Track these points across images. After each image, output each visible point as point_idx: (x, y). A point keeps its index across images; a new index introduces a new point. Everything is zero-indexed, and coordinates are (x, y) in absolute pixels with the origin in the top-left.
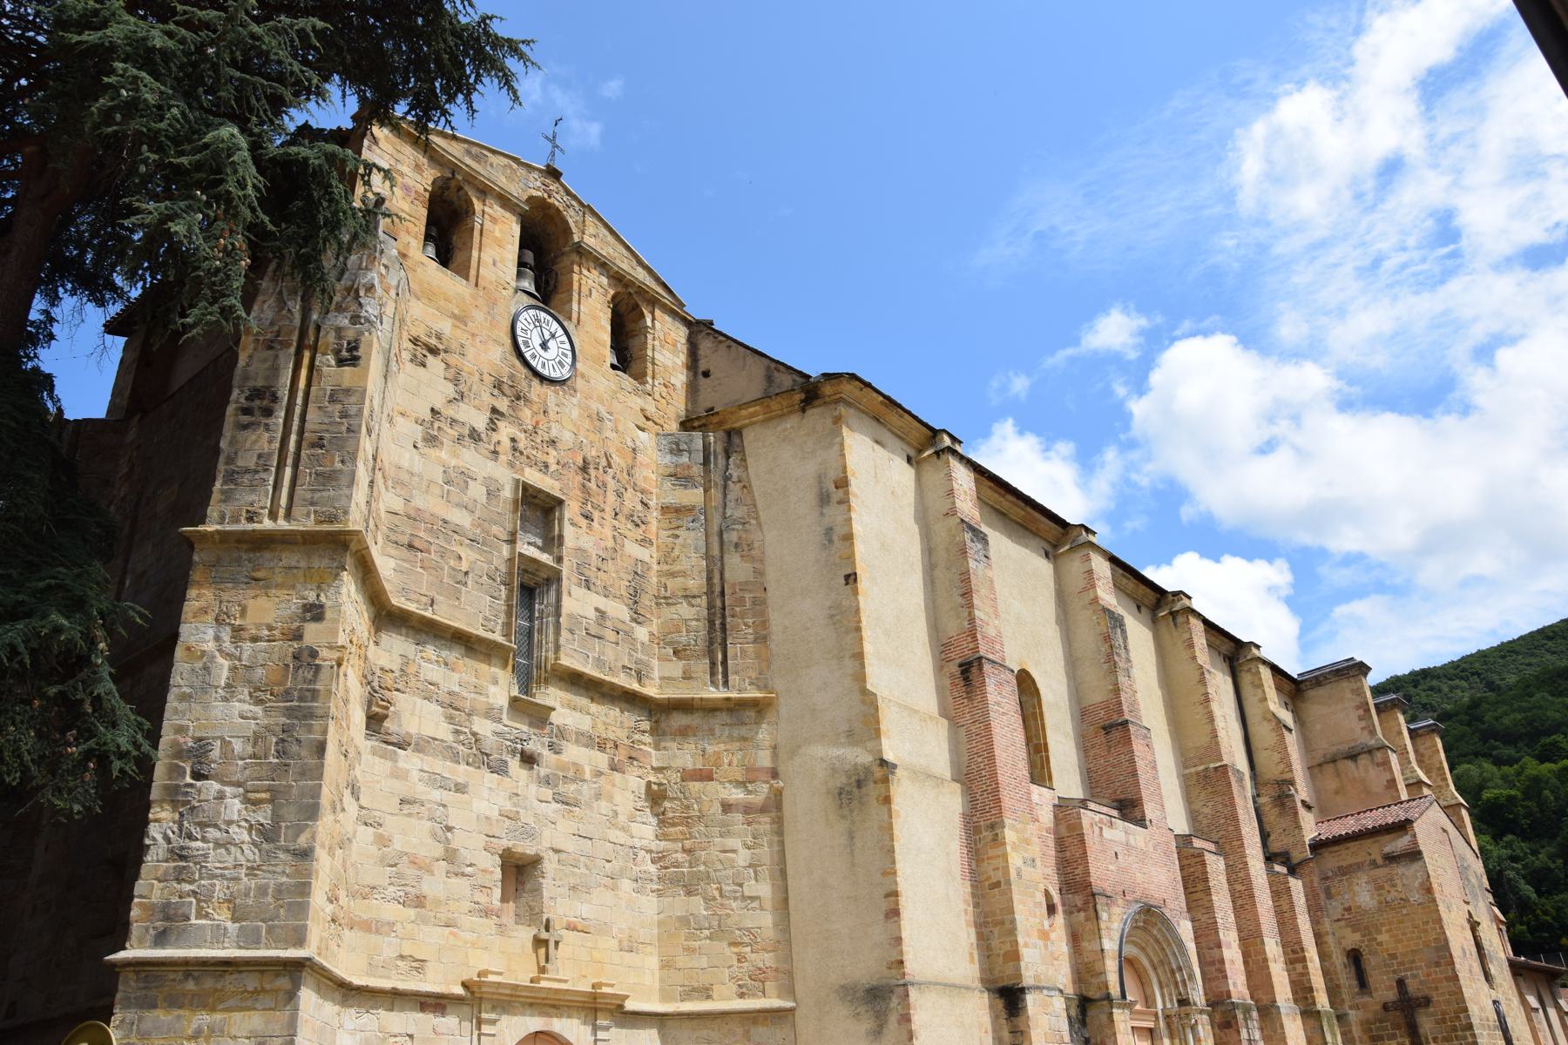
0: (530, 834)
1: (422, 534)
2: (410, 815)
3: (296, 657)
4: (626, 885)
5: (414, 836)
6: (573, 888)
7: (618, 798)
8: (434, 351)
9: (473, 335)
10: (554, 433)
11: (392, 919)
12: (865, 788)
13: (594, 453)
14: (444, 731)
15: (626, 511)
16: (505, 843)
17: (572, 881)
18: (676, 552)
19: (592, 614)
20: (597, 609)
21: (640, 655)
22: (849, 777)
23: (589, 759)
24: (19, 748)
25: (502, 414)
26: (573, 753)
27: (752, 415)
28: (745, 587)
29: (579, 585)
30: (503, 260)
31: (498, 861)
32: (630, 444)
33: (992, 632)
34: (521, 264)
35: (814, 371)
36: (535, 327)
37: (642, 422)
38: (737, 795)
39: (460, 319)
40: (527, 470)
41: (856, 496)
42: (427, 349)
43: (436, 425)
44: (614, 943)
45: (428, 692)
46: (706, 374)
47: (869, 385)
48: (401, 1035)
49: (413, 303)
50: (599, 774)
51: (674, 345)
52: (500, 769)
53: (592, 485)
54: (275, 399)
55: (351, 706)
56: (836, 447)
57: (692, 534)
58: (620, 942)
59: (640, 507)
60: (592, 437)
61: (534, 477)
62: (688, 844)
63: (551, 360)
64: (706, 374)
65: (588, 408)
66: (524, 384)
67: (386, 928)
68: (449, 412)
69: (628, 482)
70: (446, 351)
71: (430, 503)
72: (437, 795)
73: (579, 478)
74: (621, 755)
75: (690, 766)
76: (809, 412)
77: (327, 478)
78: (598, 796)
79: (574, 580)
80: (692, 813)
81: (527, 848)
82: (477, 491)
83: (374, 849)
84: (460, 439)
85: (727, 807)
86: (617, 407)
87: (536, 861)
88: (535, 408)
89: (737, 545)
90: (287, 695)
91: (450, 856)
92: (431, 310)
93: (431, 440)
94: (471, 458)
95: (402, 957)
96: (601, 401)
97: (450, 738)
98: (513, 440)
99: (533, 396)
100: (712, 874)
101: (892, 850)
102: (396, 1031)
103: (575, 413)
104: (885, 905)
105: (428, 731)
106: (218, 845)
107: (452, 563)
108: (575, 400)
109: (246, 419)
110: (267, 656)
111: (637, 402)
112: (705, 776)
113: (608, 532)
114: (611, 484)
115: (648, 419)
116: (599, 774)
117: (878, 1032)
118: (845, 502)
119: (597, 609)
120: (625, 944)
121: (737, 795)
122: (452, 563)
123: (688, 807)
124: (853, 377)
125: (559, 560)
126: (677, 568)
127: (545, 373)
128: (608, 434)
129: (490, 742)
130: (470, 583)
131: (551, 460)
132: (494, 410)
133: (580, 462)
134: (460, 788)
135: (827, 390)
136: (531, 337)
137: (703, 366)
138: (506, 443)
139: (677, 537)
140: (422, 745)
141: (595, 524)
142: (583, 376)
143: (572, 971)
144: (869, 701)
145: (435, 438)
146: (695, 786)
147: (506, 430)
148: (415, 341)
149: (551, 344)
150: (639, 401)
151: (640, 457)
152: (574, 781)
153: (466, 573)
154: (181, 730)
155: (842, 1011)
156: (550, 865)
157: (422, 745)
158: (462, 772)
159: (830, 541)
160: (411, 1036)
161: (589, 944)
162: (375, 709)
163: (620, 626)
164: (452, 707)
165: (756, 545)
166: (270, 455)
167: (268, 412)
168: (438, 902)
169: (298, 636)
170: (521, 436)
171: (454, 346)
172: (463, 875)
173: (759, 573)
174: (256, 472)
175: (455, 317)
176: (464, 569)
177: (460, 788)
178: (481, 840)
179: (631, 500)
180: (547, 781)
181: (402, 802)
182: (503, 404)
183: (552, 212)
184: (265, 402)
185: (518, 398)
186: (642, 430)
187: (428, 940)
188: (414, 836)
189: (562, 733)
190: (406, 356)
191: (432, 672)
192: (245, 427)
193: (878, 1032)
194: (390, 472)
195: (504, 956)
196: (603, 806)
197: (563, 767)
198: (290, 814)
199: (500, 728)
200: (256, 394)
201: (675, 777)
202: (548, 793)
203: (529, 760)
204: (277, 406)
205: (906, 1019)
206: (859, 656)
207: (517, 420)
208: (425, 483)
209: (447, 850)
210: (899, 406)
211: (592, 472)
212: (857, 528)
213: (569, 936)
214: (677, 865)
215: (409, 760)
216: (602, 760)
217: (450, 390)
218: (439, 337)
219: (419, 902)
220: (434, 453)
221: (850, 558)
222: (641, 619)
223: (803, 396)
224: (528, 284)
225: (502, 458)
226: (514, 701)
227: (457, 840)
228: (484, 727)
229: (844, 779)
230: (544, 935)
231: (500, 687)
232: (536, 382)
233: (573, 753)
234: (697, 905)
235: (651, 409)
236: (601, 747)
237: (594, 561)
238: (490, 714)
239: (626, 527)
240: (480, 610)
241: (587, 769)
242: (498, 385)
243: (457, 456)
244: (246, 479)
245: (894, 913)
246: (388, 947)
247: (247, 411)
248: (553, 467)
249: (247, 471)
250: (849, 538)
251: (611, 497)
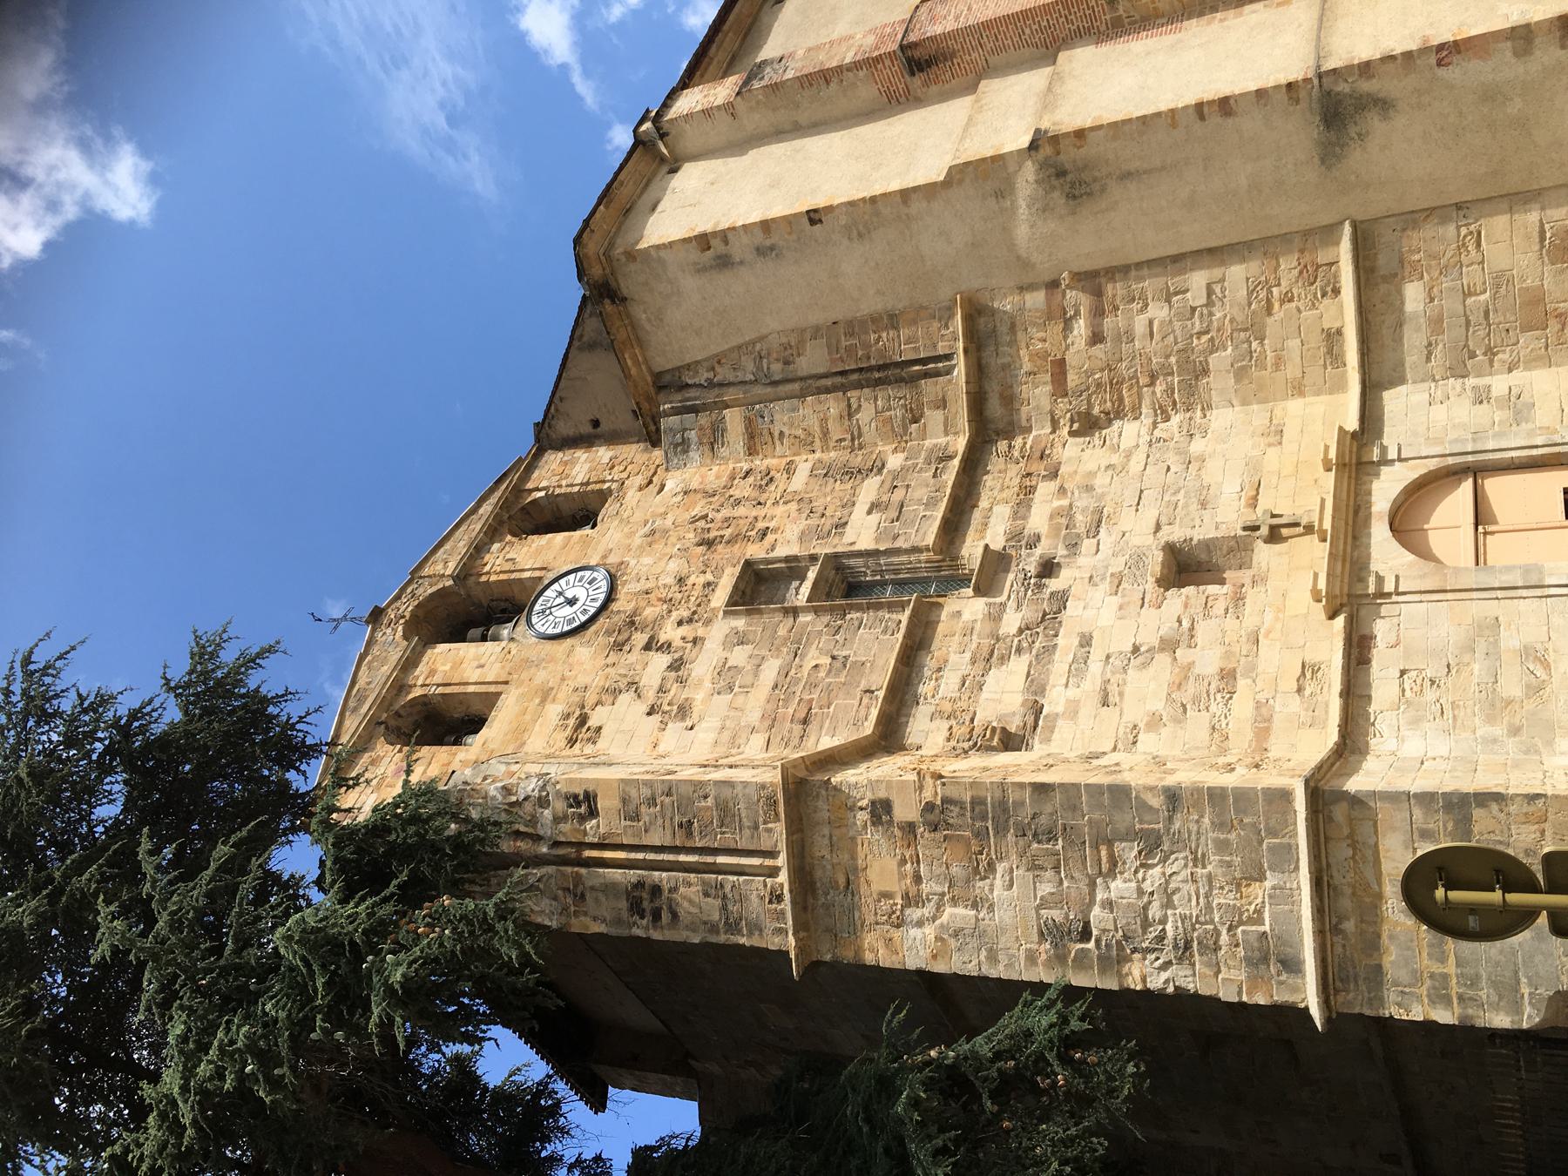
0: (1138, 559)
1: (791, 711)
2: (1121, 694)
3: (935, 828)
4: (1197, 446)
5: (1147, 689)
6: (1203, 505)
7: (1091, 466)
8: (583, 720)
9: (563, 679)
10: (670, 580)
11: (1252, 704)
12: (1068, 167)
13: (691, 535)
14: (1019, 666)
15: (755, 494)
16: (1150, 585)
17: (1194, 506)
18: (799, 432)
19: (875, 517)
20: (869, 512)
21: (921, 460)
22: (1053, 188)
23: (1045, 501)
24: (1062, 1141)
25: (652, 638)
26: (1038, 520)
27: (636, 363)
28: (833, 348)
29: (842, 534)
30: (477, 658)
31: (1173, 591)
32: (679, 498)
33: (871, 40)
34: (484, 639)
35: (576, 292)
36: (552, 614)
37: (653, 488)
38: (1081, 328)
39: (546, 695)
40: (713, 604)
41: (717, 223)
42: (581, 727)
43: (667, 708)
44: (1272, 452)
45: (973, 685)
46: (596, 423)
47: (587, 222)
48: (1401, 685)
49: (528, 748)
50: (1062, 490)
51: (566, 463)
52: (1061, 599)
53: (727, 533)
54: (640, 885)
55: (991, 765)
56: (662, 254)
57: (777, 417)
58: (1270, 445)
59: (751, 479)
60: (673, 539)
61: (720, 597)
62: (1143, 380)
63: (586, 593)
64: (596, 423)
65: (640, 547)
66: (616, 619)
67: (1264, 710)
68: (650, 696)
69: (722, 494)
70: (583, 707)
71: (755, 704)
72: (1095, 666)
73: (720, 548)
74: (1039, 468)
75: (1049, 388)
76: (625, 292)
77: (726, 812)
78: (1089, 488)
79: (836, 541)
80: (1106, 379)
81: (1155, 561)
82: (739, 656)
83: (1165, 731)
84: (681, 681)
85: (1096, 338)
86: (639, 516)
87: (1171, 550)
88: (642, 604)
89: (787, 363)
90: (981, 835)
91: (1169, 645)
92: (537, 728)
93: (683, 711)
94: (702, 667)
95: (1300, 690)
96: (632, 534)
97: (1026, 658)
98: (680, 623)
99: (630, 607)
100: (1180, 346)
101: (1143, 119)
102: (1397, 690)
103: (646, 560)
104: (1215, 119)
105: (1019, 681)
106: (1169, 904)
107: (822, 674)
108: (633, 562)
109: (665, 917)
110: (937, 863)
111: (632, 496)
112: (1060, 368)
113: (781, 509)
114: (725, 513)
115: (650, 482)
116: (1062, 490)
117: (1383, 105)
118: (724, 235)
119: (869, 512)
120: (1271, 439)
121: (1081, 328)
122: (822, 674)
123: (1099, 385)
124: (577, 241)
125: (813, 558)
126: (817, 428)
127: (602, 597)
128: (669, 522)
129: (1029, 613)
130: (845, 653)
131: (702, 580)
132: (647, 647)
133: (702, 549)
134: (1086, 641)
135: (596, 272)
136: (564, 617)
137: (587, 429)
138: (685, 630)
139: (781, 433)
140: (1036, 688)
141: (772, 525)
142: (604, 557)
143: (1310, 493)
144: (959, 174)
146: (1072, 379)
147: (670, 632)
148: (572, 742)
149: (569, 595)
150: (630, 494)
151: (694, 485)
152: (1071, 517)
153: (833, 658)
154: (1031, 958)
155: (1356, 158)
156: (1175, 534)
157: (1036, 688)
158: (1067, 641)
159: (772, 248)
160: (1403, 673)
161: (1274, 480)
162: (995, 742)
163: (887, 485)
164: (989, 658)
165: (784, 340)
166: (704, 883)
167: (656, 890)
168: (1228, 655)
169: (910, 828)
170: (675, 615)
171: (576, 698)
172: (1192, 629)
173: (816, 332)
174: (725, 897)
175: (543, 701)
177: (1086, 641)
179: (743, 489)
180: (1073, 547)
181: (1105, 704)
182: (640, 639)
183: (421, 613)
184: (645, 895)
185: (633, 623)
186: (662, 487)
187: (1277, 662)
188: (1147, 689)
189: (1015, 536)
190: (589, 749)
191: (950, 683)
192: (675, 915)
193: (1383, 105)
194: (721, 750)
196: (1101, 481)
197: (1055, 530)
198: (1124, 820)
199: (1012, 604)
200: (636, 908)
201: (1062, 404)
202: (1088, 545)
203: (1048, 568)
204: (648, 882)
205: (1366, 68)
206: (905, 195)
207: (658, 622)
208: (732, 713)
209: (1162, 650)
210: (609, 186)
211: (712, 535)
212: (755, 217)
213: (1264, 503)
214: (1170, 391)
215: (1054, 702)
216: (1045, 489)
217: (625, 698)
218: (567, 716)
220: (697, 708)
221: (789, 220)
222: (878, 463)
223: (607, 301)
224: (505, 632)
225: (700, 633)
226: (980, 591)
227: (1149, 639)
228: (1011, 622)
229: (1056, 194)
230: (1264, 531)
231: (965, 608)
232: (614, 607)
233: (1038, 520)
234: (1220, 360)
235: (639, 480)
236: (1031, 490)
237: (814, 521)
238: (995, 616)
239: (773, 492)
240: (876, 641)
241: (1056, 504)
242: (619, 646)
243: (700, 682)
244: (734, 908)
245: (1225, 105)
247: (656, 916)
248: (709, 577)
249: (724, 908)
250: (766, 225)
251: (741, 511)
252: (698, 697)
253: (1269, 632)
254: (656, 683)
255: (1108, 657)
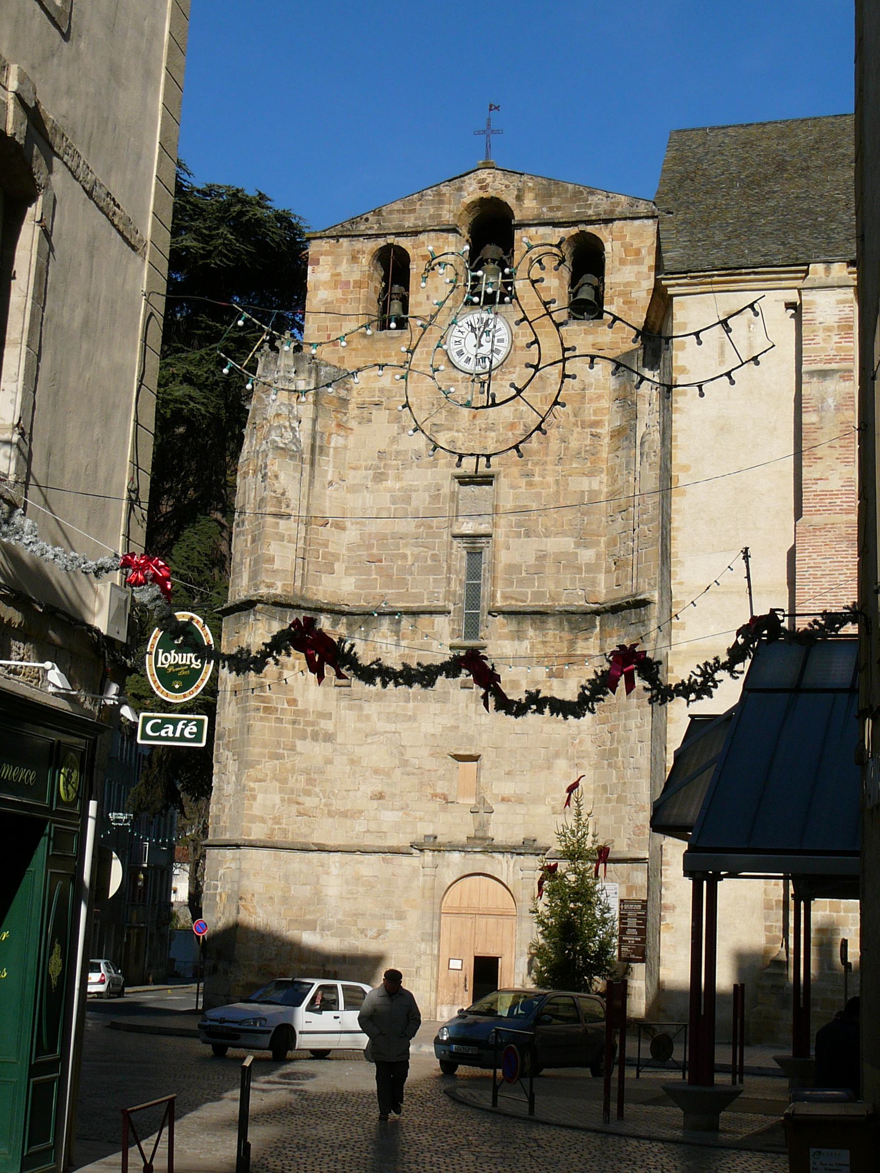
2: (372, 743)
6: (508, 773)
17: (507, 769)
44: (549, 809)
58: (553, 807)
91: (405, 763)
93: (380, 477)
102: (366, 874)
113: (550, 479)
141: (537, 479)
145: (382, 473)
161: (523, 812)
168: (394, 795)
172: (413, 774)
176: (409, 563)
177: (412, 718)
178: (425, 752)
187: (389, 817)
195: (456, 825)
219: (380, 796)
227: (409, 754)
243: (398, 478)
246: (360, 826)
252: (389, 484)
253: (407, 815)
254: (401, 448)
255: (400, 733)
